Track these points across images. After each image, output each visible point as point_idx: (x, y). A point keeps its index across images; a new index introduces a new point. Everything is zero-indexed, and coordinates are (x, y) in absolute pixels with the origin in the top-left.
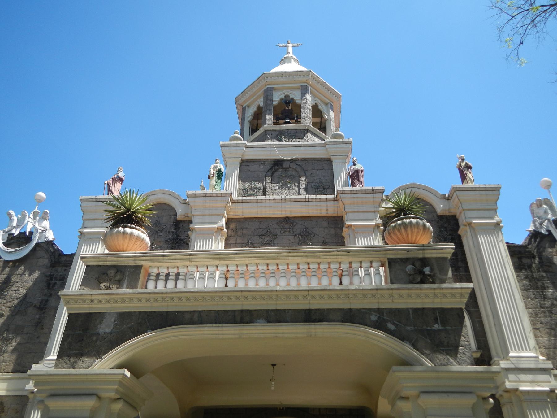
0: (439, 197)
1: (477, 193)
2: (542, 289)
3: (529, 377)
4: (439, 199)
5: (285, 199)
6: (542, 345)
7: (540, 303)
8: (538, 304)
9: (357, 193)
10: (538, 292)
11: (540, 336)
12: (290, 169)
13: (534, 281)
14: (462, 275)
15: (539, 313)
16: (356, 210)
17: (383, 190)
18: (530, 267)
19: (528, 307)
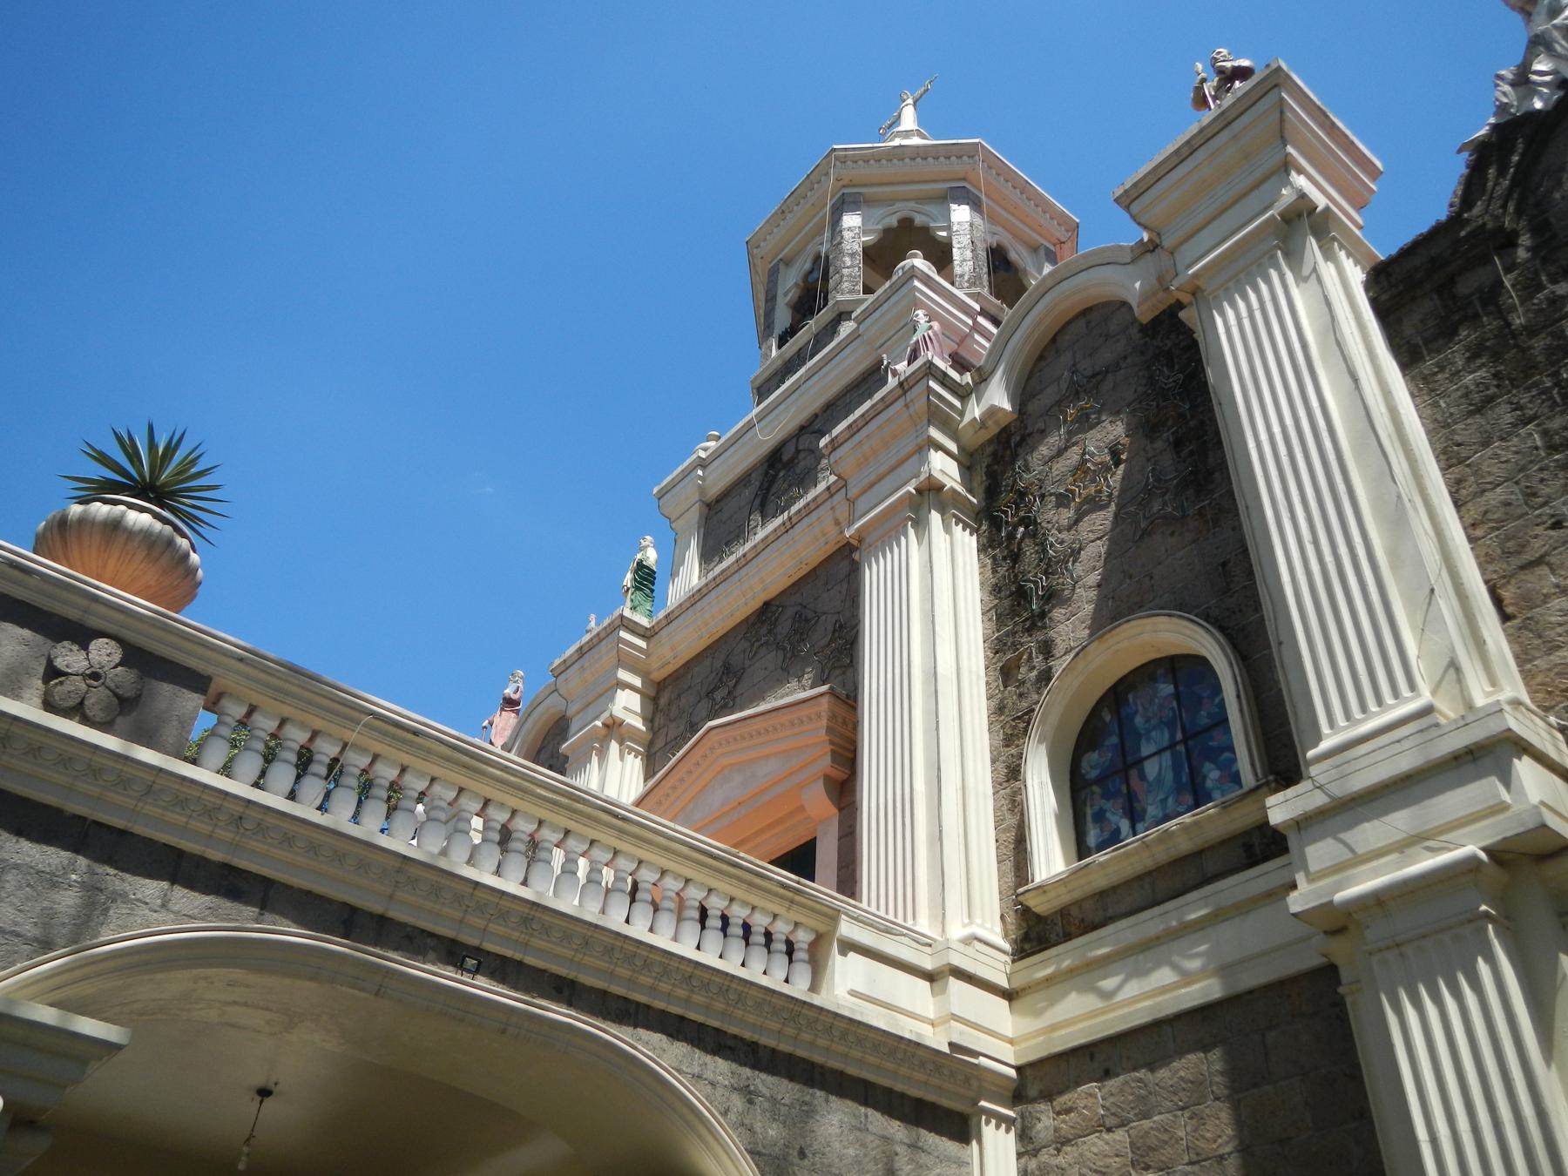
0: (1128, 260)
1: (1201, 155)
2: (1552, 364)
3: (1398, 822)
4: (1130, 267)
5: (744, 555)
6: (1559, 630)
7: (1545, 433)
8: (1539, 443)
9: (867, 423)
10: (1528, 389)
11: (1553, 591)
12: (802, 455)
13: (1516, 346)
14: (1221, 495)
15: (1542, 480)
16: (873, 477)
17: (925, 364)
18: (1492, 295)
19: (1490, 479)
